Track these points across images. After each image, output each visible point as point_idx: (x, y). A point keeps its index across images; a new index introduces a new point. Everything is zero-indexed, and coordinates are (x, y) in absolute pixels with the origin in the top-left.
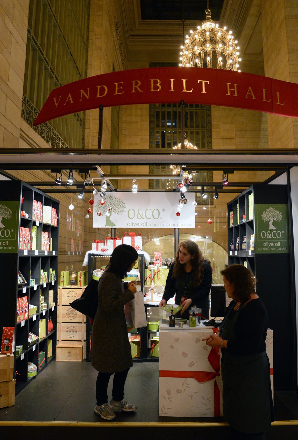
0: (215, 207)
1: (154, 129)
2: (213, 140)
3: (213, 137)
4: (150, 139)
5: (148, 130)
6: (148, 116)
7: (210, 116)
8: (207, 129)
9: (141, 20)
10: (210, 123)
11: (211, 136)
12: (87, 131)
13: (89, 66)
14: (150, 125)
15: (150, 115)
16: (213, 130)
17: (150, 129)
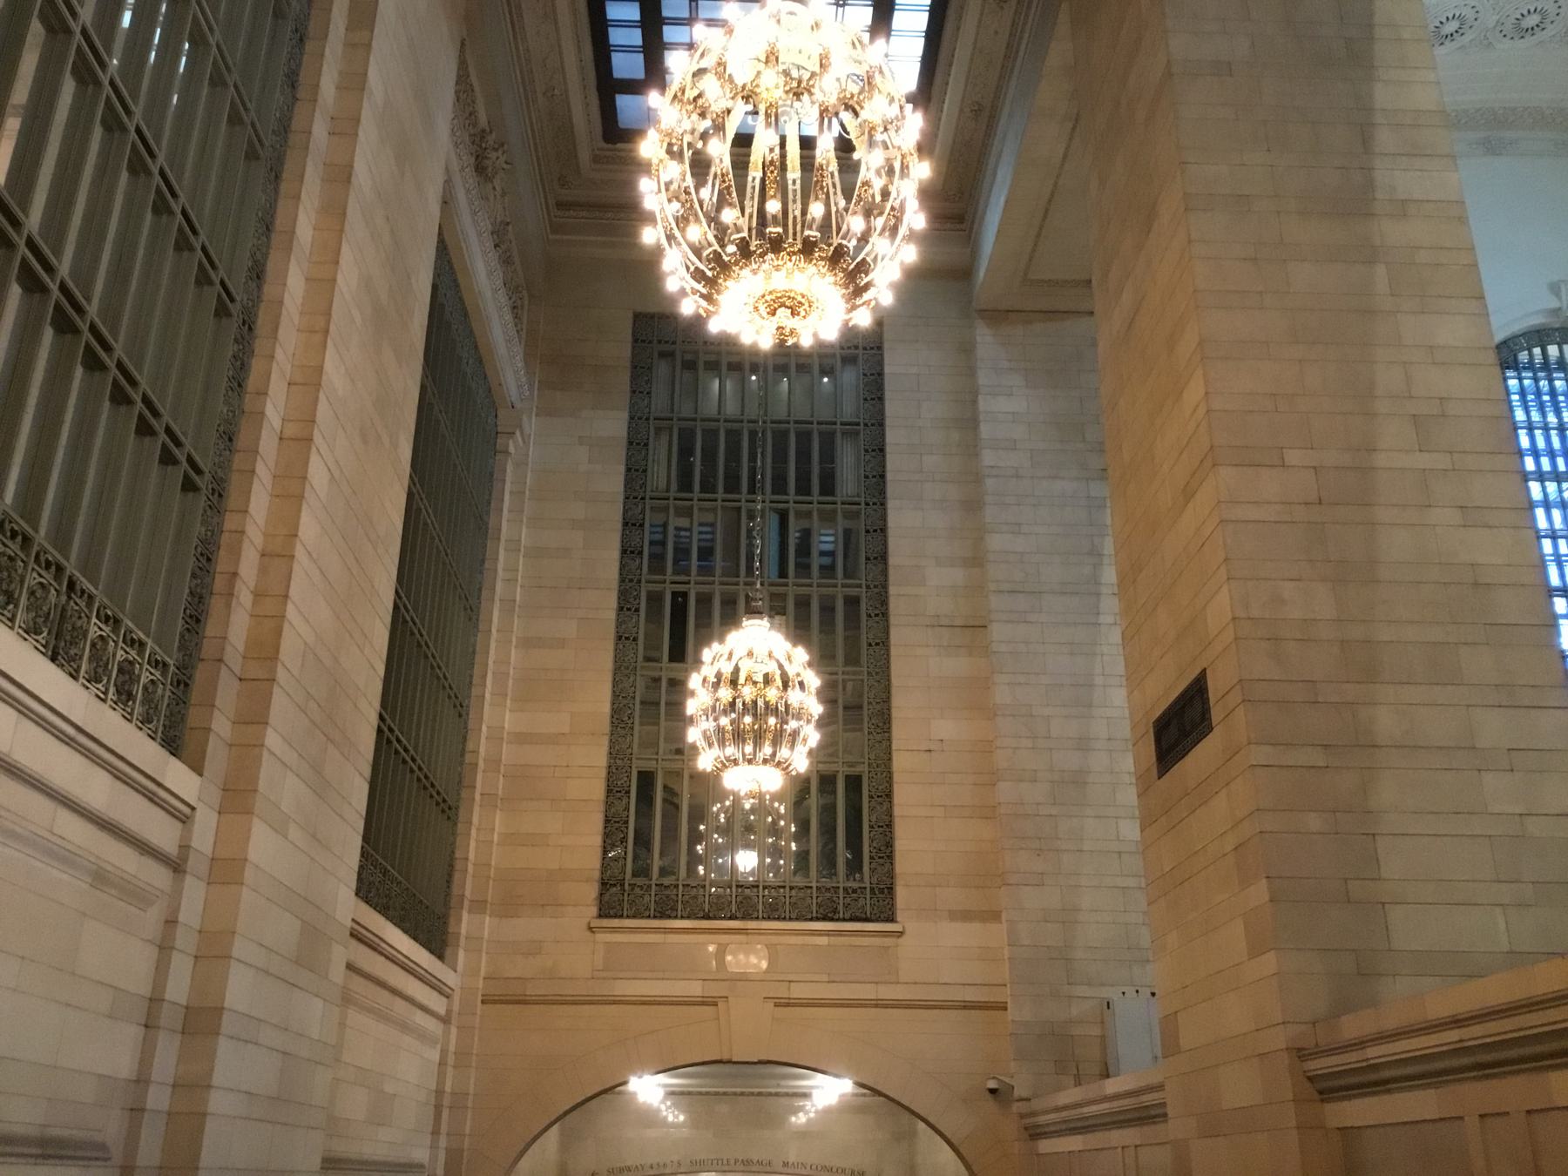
0: (901, 934)
1: (639, 581)
2: (893, 633)
3: (893, 620)
4: (619, 624)
5: (615, 584)
6: (619, 526)
7: (884, 530)
8: (868, 587)
9: (603, 145)
10: (882, 557)
11: (885, 615)
12: (230, 522)
13: (276, 239)
14: (622, 567)
15: (625, 524)
16: (892, 590)
17: (622, 580)
